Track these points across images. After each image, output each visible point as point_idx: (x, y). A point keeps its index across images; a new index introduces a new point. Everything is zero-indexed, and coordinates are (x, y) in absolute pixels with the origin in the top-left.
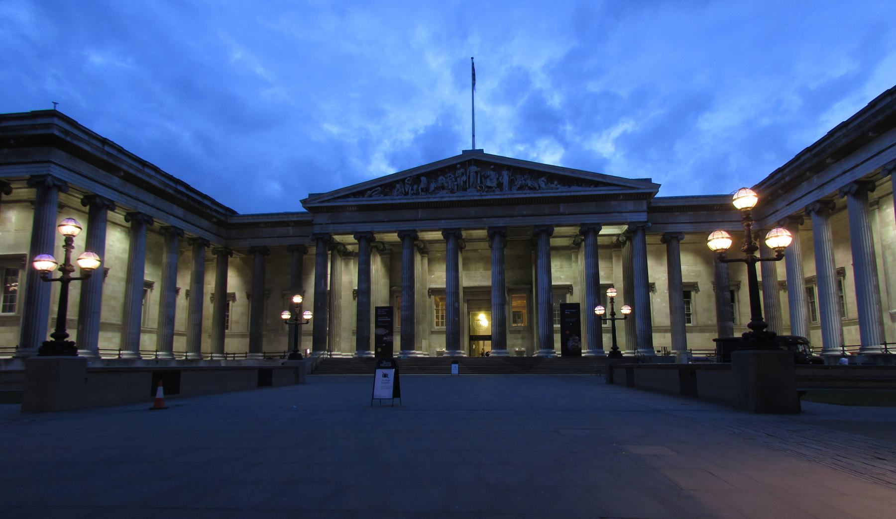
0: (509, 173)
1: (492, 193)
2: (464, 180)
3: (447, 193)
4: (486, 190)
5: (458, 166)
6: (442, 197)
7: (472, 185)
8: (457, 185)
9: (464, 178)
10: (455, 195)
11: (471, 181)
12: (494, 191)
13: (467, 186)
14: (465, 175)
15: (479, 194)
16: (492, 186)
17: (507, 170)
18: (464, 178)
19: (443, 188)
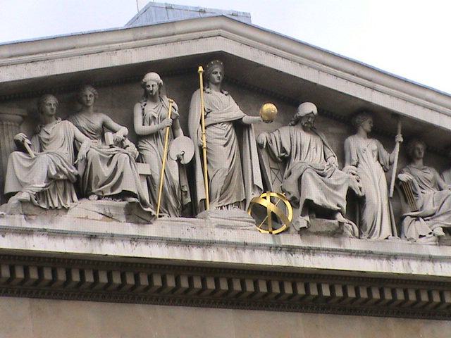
0: (384, 153)
1: (327, 243)
2: (187, 160)
3: (108, 217)
4: (304, 221)
5: (153, 78)
6: (92, 237)
7: (224, 193)
8: (149, 179)
9: (184, 147)
10: (151, 230)
11: (223, 158)
12: (338, 233)
13: (202, 194)
14: (180, 131)
15: (263, 237)
16: (334, 207)
17: (371, 135)
18: (184, 147)
19: (82, 186)
